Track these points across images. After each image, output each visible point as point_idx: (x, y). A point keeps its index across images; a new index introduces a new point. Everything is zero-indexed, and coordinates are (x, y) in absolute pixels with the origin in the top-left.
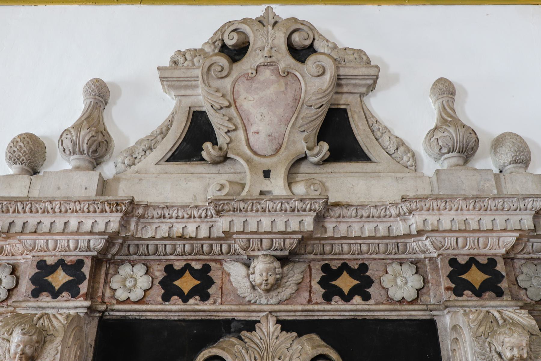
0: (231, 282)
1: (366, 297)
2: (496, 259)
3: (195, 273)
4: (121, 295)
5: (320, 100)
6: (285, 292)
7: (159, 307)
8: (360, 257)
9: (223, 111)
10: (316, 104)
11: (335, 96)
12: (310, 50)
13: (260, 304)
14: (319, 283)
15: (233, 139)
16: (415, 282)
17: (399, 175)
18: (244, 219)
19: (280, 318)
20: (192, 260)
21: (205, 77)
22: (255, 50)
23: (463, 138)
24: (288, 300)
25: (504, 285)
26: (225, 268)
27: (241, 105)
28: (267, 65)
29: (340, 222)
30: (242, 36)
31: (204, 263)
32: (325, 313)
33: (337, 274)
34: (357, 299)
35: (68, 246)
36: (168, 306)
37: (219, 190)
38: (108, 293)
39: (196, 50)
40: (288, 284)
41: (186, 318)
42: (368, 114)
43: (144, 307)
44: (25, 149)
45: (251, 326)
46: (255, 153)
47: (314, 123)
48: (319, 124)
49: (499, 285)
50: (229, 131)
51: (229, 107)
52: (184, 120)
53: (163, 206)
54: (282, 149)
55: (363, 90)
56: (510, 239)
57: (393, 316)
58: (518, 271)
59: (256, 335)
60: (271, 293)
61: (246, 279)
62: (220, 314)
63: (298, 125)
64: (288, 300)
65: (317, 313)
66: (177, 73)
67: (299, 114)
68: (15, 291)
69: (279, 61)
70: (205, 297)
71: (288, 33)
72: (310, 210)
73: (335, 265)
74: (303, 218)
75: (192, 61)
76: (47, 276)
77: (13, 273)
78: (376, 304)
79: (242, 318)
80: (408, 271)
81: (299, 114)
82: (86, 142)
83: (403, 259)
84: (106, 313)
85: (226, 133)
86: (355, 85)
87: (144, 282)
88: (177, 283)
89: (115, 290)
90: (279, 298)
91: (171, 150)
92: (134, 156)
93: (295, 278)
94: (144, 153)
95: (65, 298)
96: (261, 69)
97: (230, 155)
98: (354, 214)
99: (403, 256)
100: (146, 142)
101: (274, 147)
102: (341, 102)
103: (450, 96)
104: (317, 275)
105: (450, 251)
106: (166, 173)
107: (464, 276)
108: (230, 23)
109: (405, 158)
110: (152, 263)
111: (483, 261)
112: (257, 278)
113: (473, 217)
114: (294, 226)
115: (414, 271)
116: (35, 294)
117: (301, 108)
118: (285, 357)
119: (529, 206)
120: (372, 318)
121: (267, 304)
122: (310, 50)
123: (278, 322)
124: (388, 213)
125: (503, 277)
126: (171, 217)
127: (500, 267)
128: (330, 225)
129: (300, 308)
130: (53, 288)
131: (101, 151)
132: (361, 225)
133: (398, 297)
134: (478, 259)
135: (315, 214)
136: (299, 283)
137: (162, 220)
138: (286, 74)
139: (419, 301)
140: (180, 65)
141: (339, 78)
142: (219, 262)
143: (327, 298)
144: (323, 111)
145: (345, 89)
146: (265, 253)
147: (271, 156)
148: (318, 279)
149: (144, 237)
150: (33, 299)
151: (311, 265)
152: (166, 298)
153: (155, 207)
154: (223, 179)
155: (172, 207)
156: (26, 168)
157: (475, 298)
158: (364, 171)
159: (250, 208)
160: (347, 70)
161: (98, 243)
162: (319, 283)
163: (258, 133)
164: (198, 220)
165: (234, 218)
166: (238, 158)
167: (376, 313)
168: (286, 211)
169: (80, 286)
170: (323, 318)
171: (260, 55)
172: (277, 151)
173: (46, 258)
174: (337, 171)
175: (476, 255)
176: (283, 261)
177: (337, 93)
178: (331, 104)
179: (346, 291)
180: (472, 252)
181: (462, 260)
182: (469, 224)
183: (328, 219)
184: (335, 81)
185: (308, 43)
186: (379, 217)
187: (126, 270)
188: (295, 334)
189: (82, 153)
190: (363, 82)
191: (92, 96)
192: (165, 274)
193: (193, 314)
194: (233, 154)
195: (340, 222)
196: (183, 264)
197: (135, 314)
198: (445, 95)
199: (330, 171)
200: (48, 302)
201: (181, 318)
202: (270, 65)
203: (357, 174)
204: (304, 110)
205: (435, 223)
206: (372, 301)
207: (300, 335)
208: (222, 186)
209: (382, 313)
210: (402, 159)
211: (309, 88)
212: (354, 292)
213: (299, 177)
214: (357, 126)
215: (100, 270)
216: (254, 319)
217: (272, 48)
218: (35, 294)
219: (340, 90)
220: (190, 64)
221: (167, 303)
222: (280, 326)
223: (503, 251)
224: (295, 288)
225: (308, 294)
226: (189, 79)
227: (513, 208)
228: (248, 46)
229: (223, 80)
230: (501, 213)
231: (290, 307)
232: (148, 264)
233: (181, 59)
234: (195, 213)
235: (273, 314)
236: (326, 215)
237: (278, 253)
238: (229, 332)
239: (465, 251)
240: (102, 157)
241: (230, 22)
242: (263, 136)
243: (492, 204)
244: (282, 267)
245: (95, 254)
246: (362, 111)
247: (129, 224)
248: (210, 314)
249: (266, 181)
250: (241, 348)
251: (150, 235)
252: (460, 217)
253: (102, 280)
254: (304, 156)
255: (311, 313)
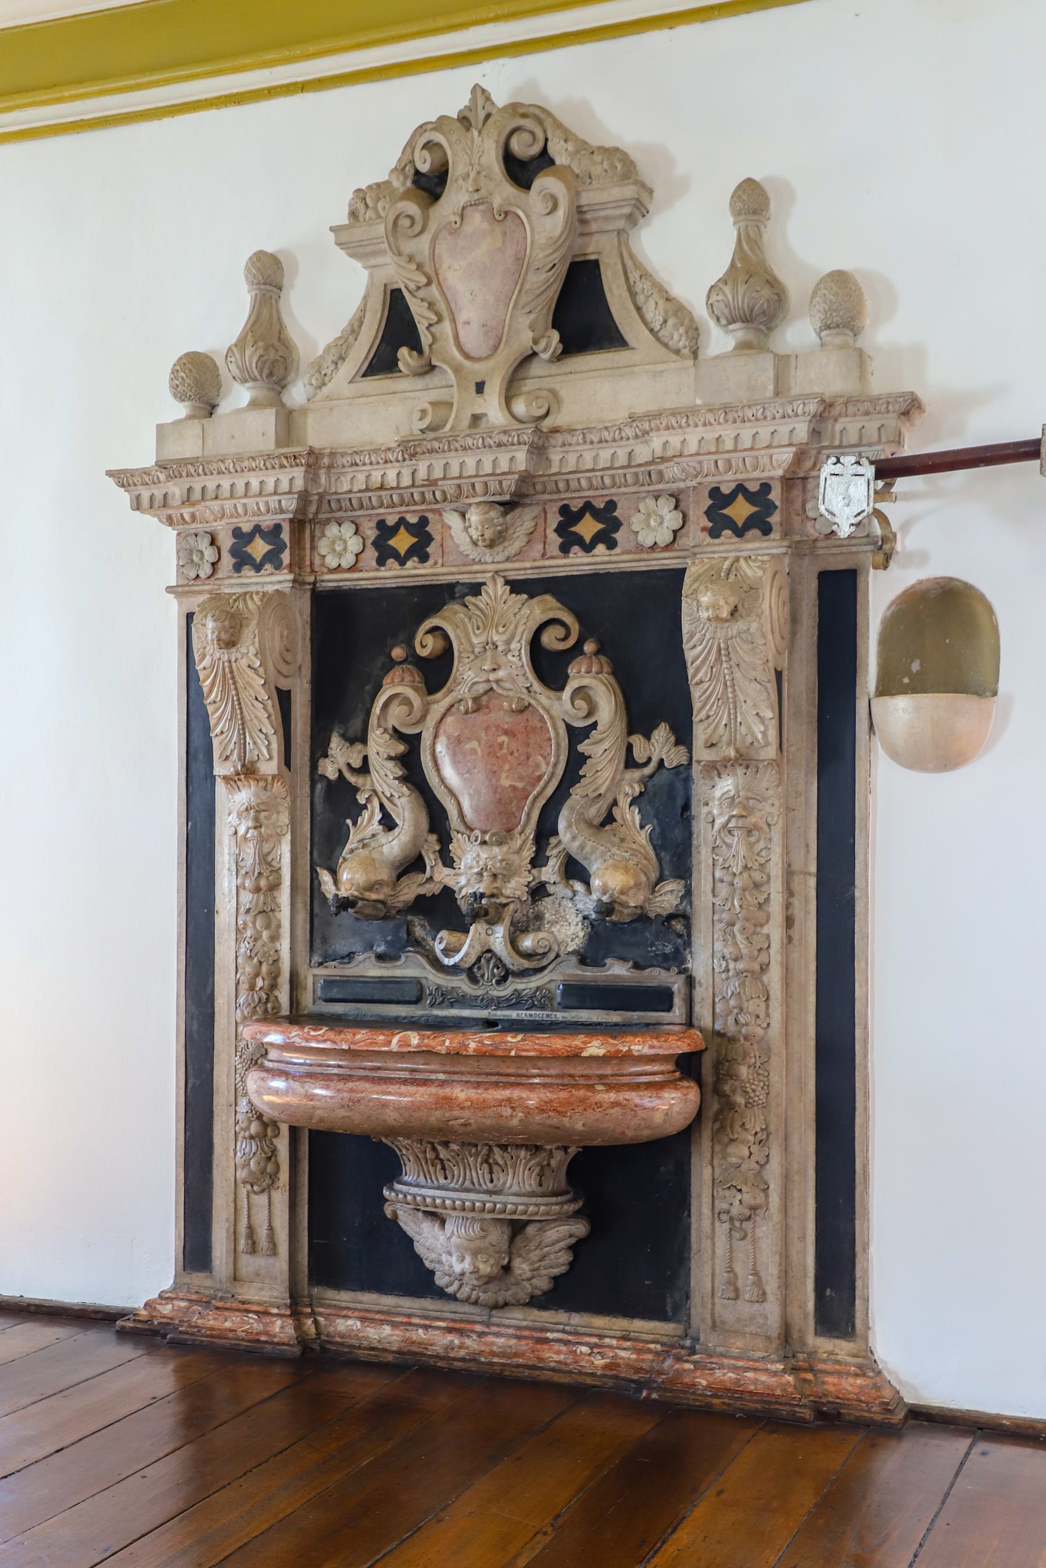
0: (452, 537)
1: (612, 545)
2: (772, 483)
3: (411, 529)
4: (332, 562)
5: (549, 259)
6: (513, 547)
7: (371, 574)
8: (605, 492)
9: (421, 294)
10: (544, 266)
11: (580, 241)
12: (544, 160)
13: (486, 563)
14: (556, 530)
15: (438, 336)
16: (673, 519)
17: (660, 367)
18: (444, 462)
19: (510, 578)
20: (407, 512)
21: (391, 239)
22: (457, 180)
23: (743, 301)
24: (519, 555)
25: (775, 519)
26: (447, 521)
27: (445, 279)
28: (475, 204)
29: (567, 452)
30: (438, 154)
31: (421, 514)
32: (561, 569)
33: (578, 517)
34: (601, 548)
35: (259, 509)
36: (383, 573)
37: (421, 419)
38: (317, 561)
39: (378, 185)
40: (516, 535)
41: (405, 585)
42: (629, 264)
43: (355, 575)
44: (188, 381)
45: (476, 589)
46: (467, 356)
47: (543, 297)
48: (552, 298)
49: (768, 520)
50: (430, 325)
51: (429, 284)
52: (379, 307)
53: (349, 451)
54: (502, 345)
55: (621, 224)
56: (785, 456)
57: (642, 566)
58: (810, 495)
59: (482, 601)
60: (496, 549)
61: (465, 535)
62: (441, 578)
63: (522, 303)
64: (519, 555)
65: (551, 570)
66: (358, 234)
67: (523, 284)
68: (219, 564)
69: (491, 194)
70: (424, 558)
71: (502, 139)
72: (520, 444)
73: (576, 506)
74: (514, 454)
75: (375, 209)
76: (246, 546)
77: (213, 542)
78: (623, 553)
79: (468, 581)
80: (665, 507)
81: (523, 284)
82: (254, 365)
83: (661, 490)
84: (318, 585)
85: (428, 328)
86: (607, 219)
87: (354, 544)
88: (392, 542)
89: (324, 557)
90: (506, 553)
91: (366, 358)
92: (323, 373)
93: (524, 527)
94: (333, 366)
95: (268, 572)
96: (469, 211)
97: (434, 363)
98: (581, 441)
99: (660, 486)
100: (333, 350)
101: (491, 343)
102: (590, 250)
103: (749, 217)
104: (554, 519)
105: (710, 479)
106: (363, 396)
107: (725, 511)
108: (422, 129)
109: (676, 337)
110: (361, 519)
111: (753, 487)
112: (475, 534)
113: (728, 432)
114: (504, 466)
115: (672, 506)
116: (238, 568)
117: (526, 273)
118: (510, 624)
119: (800, 411)
120: (617, 571)
121: (493, 562)
122: (544, 160)
123: (507, 582)
124: (623, 435)
125: (776, 507)
126: (364, 464)
127: (775, 496)
128: (555, 457)
129: (528, 565)
130: (254, 559)
131: (279, 372)
132: (594, 453)
133: (649, 542)
134: (748, 485)
135: (526, 447)
136: (531, 533)
137: (355, 468)
138: (503, 215)
139: (676, 545)
140: (361, 219)
141: (580, 210)
142: (438, 512)
143: (565, 549)
144: (563, 270)
145: (594, 227)
146: (482, 499)
147: (488, 357)
148: (555, 526)
149: (340, 491)
150: (236, 575)
151: (547, 507)
152: (381, 562)
153: (343, 455)
154: (423, 400)
155: (362, 451)
156: (198, 405)
157: (736, 539)
158: (615, 365)
159: (446, 447)
160: (591, 194)
161: (290, 504)
162: (556, 530)
163: (468, 323)
164: (397, 464)
165: (433, 461)
166: (445, 367)
167: (621, 565)
168: (490, 447)
169: (282, 556)
170: (560, 574)
171: (464, 189)
172: (496, 348)
173: (240, 525)
174: (578, 369)
175: (745, 480)
176: (509, 506)
177: (582, 235)
178: (574, 256)
179: (588, 539)
180: (739, 476)
181: (726, 490)
182: (723, 441)
183: (551, 450)
184: (576, 217)
185: (535, 150)
186: (614, 440)
187: (332, 530)
188: (525, 596)
189: (255, 380)
190: (617, 212)
191: (255, 287)
192: (377, 532)
193: (411, 579)
194: (438, 360)
195: (567, 452)
196: (396, 518)
197: (348, 583)
198: (741, 218)
199: (568, 370)
200: (250, 577)
201: (400, 585)
202: (480, 204)
203: (603, 373)
204: (530, 275)
205: (678, 445)
206: (617, 550)
207: (532, 596)
208: (424, 412)
209: (628, 565)
210: (672, 338)
211: (537, 237)
212: (598, 538)
213: (529, 385)
214: (611, 290)
215: (304, 532)
216: (481, 580)
217: (479, 173)
218: (238, 568)
219: (586, 230)
220: (374, 217)
221: (383, 568)
222: (508, 588)
223: (780, 472)
224: (526, 540)
225: (542, 545)
226: (375, 241)
227: (778, 416)
228: (447, 171)
229: (417, 239)
230: (764, 423)
231: (517, 565)
232: (358, 521)
233: (361, 207)
234: (390, 455)
235: (502, 574)
236: (546, 445)
237: (498, 498)
238: (453, 597)
239: (729, 476)
240: (284, 378)
241: (421, 127)
242: (475, 326)
243: (749, 413)
244: (505, 514)
245: (291, 516)
246: (619, 261)
247: (319, 477)
248: (429, 578)
249: (479, 399)
250: (462, 615)
251: (346, 487)
252: (711, 435)
253: (308, 546)
254: (531, 352)
255: (544, 570)
